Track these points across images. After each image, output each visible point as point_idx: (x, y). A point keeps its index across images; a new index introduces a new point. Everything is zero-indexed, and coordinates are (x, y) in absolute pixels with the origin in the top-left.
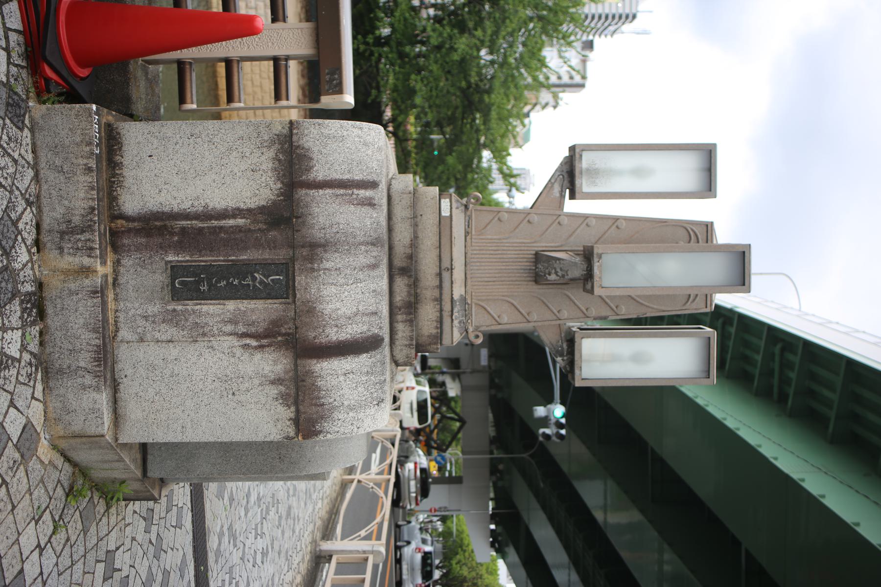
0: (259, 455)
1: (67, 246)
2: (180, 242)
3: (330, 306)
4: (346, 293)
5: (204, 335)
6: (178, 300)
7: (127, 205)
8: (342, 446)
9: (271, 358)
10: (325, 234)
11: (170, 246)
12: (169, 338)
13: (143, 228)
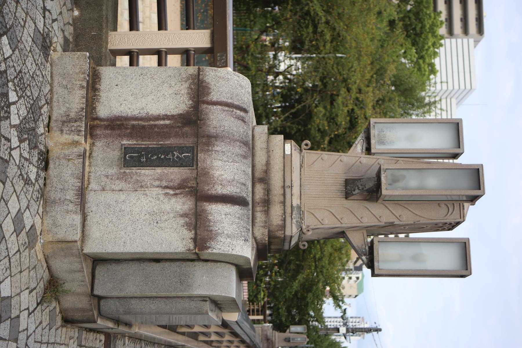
0: (167, 280)
1: (65, 129)
2: (131, 133)
3: (218, 172)
4: (228, 166)
5: (142, 187)
6: (127, 167)
7: (101, 112)
8: (220, 280)
9: (181, 201)
10: (216, 131)
11: (124, 136)
12: (120, 188)
13: (109, 125)
